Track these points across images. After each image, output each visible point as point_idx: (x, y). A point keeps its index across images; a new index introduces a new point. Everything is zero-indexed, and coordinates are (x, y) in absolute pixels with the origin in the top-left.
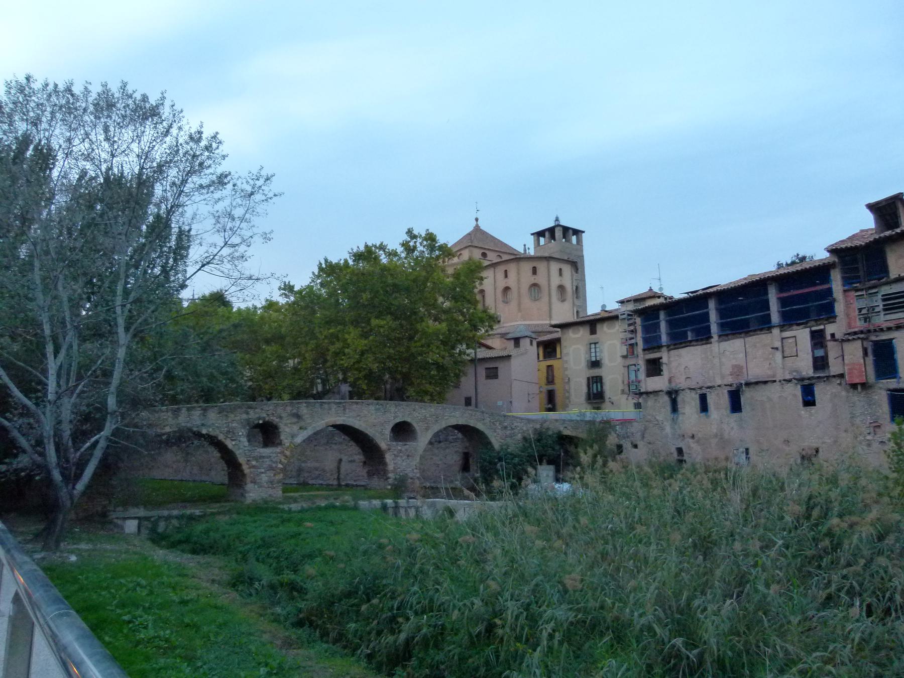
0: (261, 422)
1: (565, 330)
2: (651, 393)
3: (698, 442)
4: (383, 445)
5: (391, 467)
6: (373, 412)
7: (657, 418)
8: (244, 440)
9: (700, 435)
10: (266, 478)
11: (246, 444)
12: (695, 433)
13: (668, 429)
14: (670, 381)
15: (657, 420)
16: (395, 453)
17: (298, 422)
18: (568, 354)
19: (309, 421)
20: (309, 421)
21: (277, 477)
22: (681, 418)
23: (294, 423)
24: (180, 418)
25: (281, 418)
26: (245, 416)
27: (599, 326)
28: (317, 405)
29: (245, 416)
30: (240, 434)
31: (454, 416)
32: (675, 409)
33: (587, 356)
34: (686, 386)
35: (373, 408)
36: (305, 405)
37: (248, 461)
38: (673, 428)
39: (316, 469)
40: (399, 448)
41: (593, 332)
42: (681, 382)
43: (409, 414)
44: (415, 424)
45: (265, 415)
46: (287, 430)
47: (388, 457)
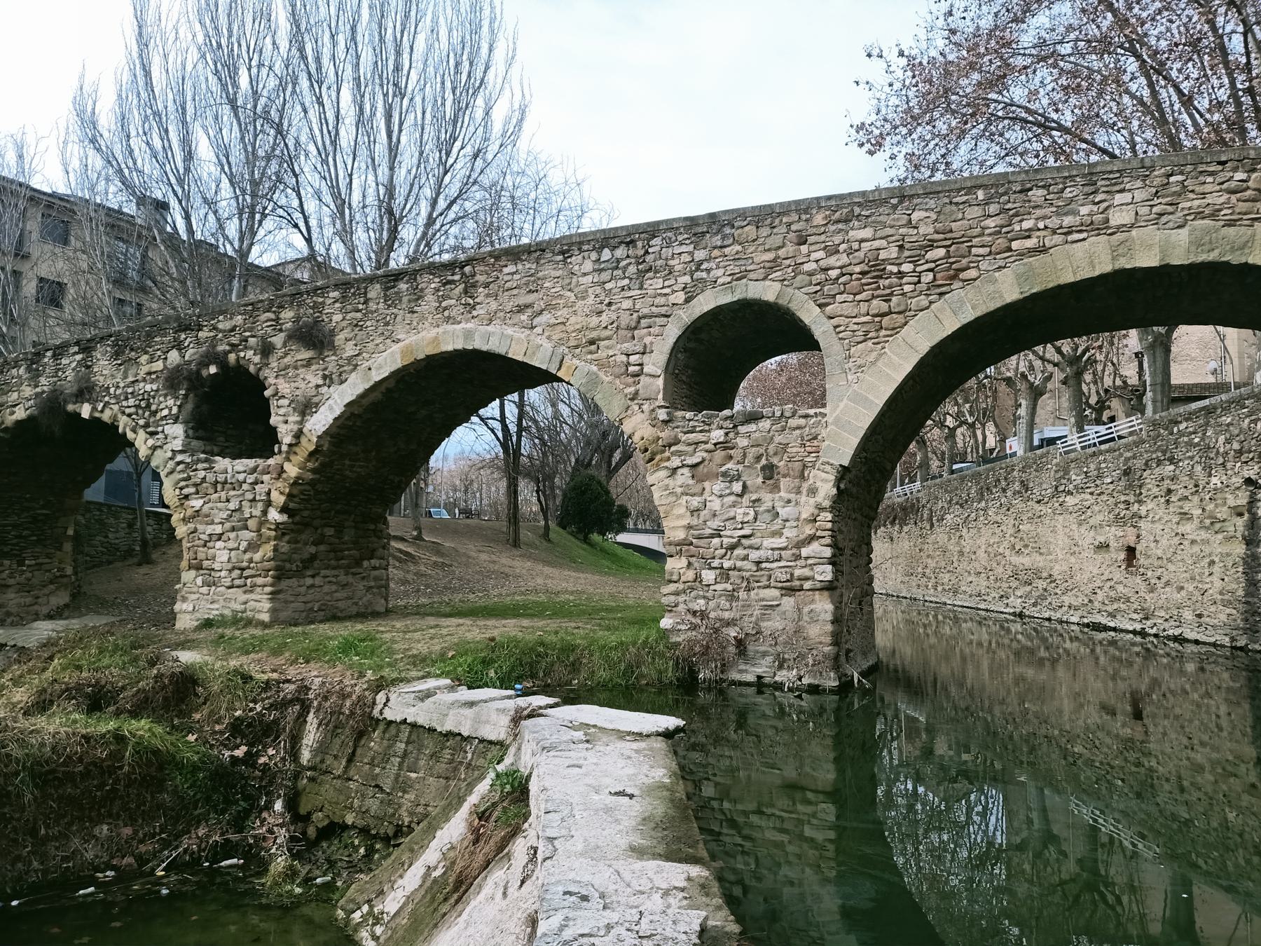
0: (213, 370)
5: (675, 527)
8: (176, 433)
10: (223, 556)
11: (178, 444)
19: (350, 350)
20: (350, 350)
21: (257, 557)
23: (308, 363)
24: (43, 380)
25: (266, 350)
26: (174, 356)
28: (375, 291)
29: (174, 356)
30: (165, 412)
31: (1100, 228)
35: (588, 266)
36: (336, 294)
37: (186, 497)
39: (1037, 573)
40: (717, 435)
43: (775, 264)
45: (222, 348)
46: (284, 387)
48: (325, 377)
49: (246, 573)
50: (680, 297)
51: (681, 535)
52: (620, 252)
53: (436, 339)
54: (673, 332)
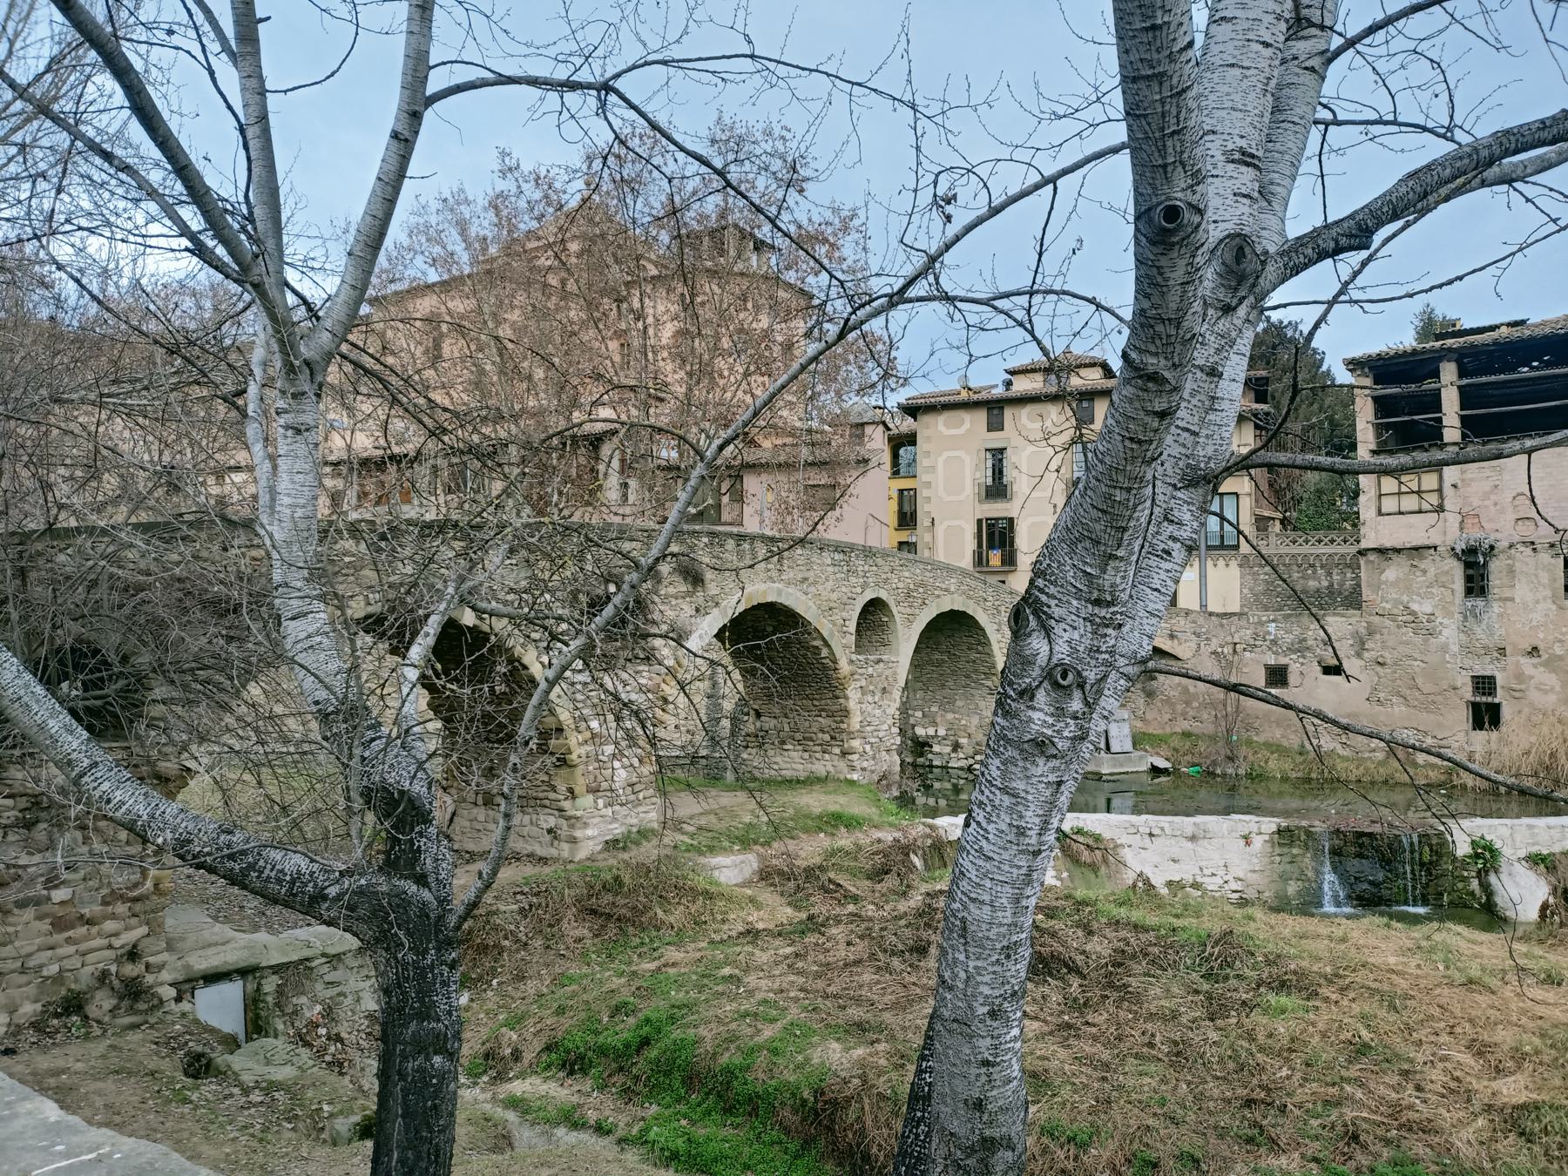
1: (926, 419)
2: (1398, 551)
3: (1546, 664)
4: (844, 667)
5: (855, 722)
6: (831, 569)
7: (1415, 607)
9: (1558, 650)
12: (1541, 646)
13: (1450, 633)
14: (1461, 529)
15: (1413, 613)
16: (863, 683)
17: (690, 594)
18: (933, 469)
20: (713, 589)
22: (1496, 608)
27: (1008, 413)
32: (1476, 584)
33: (978, 475)
34: (1516, 539)
35: (829, 561)
36: (705, 540)
38: (1464, 630)
41: (995, 425)
42: (1500, 526)
44: (895, 610)
47: (853, 694)
48: (697, 610)
49: (637, 788)
50: (859, 590)
51: (858, 727)
52: (841, 556)
53: (765, 593)
54: (858, 610)
